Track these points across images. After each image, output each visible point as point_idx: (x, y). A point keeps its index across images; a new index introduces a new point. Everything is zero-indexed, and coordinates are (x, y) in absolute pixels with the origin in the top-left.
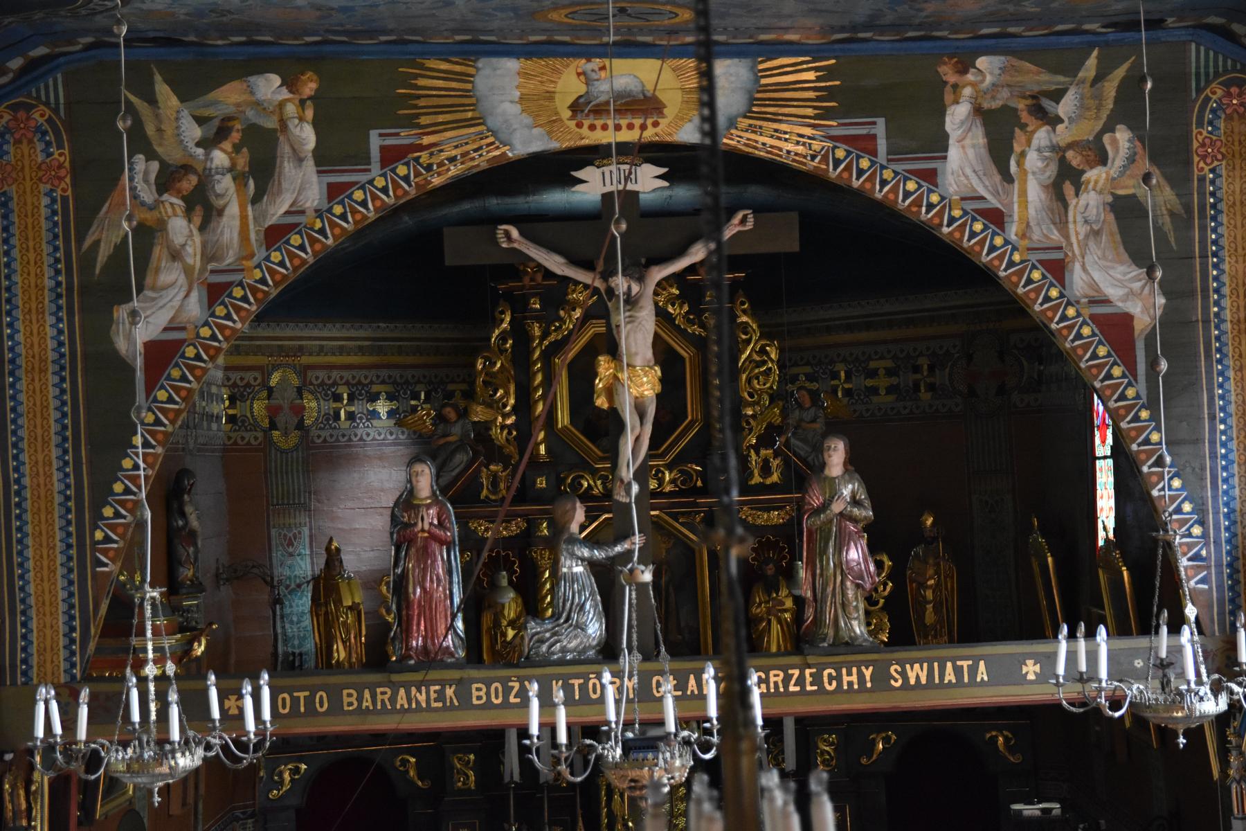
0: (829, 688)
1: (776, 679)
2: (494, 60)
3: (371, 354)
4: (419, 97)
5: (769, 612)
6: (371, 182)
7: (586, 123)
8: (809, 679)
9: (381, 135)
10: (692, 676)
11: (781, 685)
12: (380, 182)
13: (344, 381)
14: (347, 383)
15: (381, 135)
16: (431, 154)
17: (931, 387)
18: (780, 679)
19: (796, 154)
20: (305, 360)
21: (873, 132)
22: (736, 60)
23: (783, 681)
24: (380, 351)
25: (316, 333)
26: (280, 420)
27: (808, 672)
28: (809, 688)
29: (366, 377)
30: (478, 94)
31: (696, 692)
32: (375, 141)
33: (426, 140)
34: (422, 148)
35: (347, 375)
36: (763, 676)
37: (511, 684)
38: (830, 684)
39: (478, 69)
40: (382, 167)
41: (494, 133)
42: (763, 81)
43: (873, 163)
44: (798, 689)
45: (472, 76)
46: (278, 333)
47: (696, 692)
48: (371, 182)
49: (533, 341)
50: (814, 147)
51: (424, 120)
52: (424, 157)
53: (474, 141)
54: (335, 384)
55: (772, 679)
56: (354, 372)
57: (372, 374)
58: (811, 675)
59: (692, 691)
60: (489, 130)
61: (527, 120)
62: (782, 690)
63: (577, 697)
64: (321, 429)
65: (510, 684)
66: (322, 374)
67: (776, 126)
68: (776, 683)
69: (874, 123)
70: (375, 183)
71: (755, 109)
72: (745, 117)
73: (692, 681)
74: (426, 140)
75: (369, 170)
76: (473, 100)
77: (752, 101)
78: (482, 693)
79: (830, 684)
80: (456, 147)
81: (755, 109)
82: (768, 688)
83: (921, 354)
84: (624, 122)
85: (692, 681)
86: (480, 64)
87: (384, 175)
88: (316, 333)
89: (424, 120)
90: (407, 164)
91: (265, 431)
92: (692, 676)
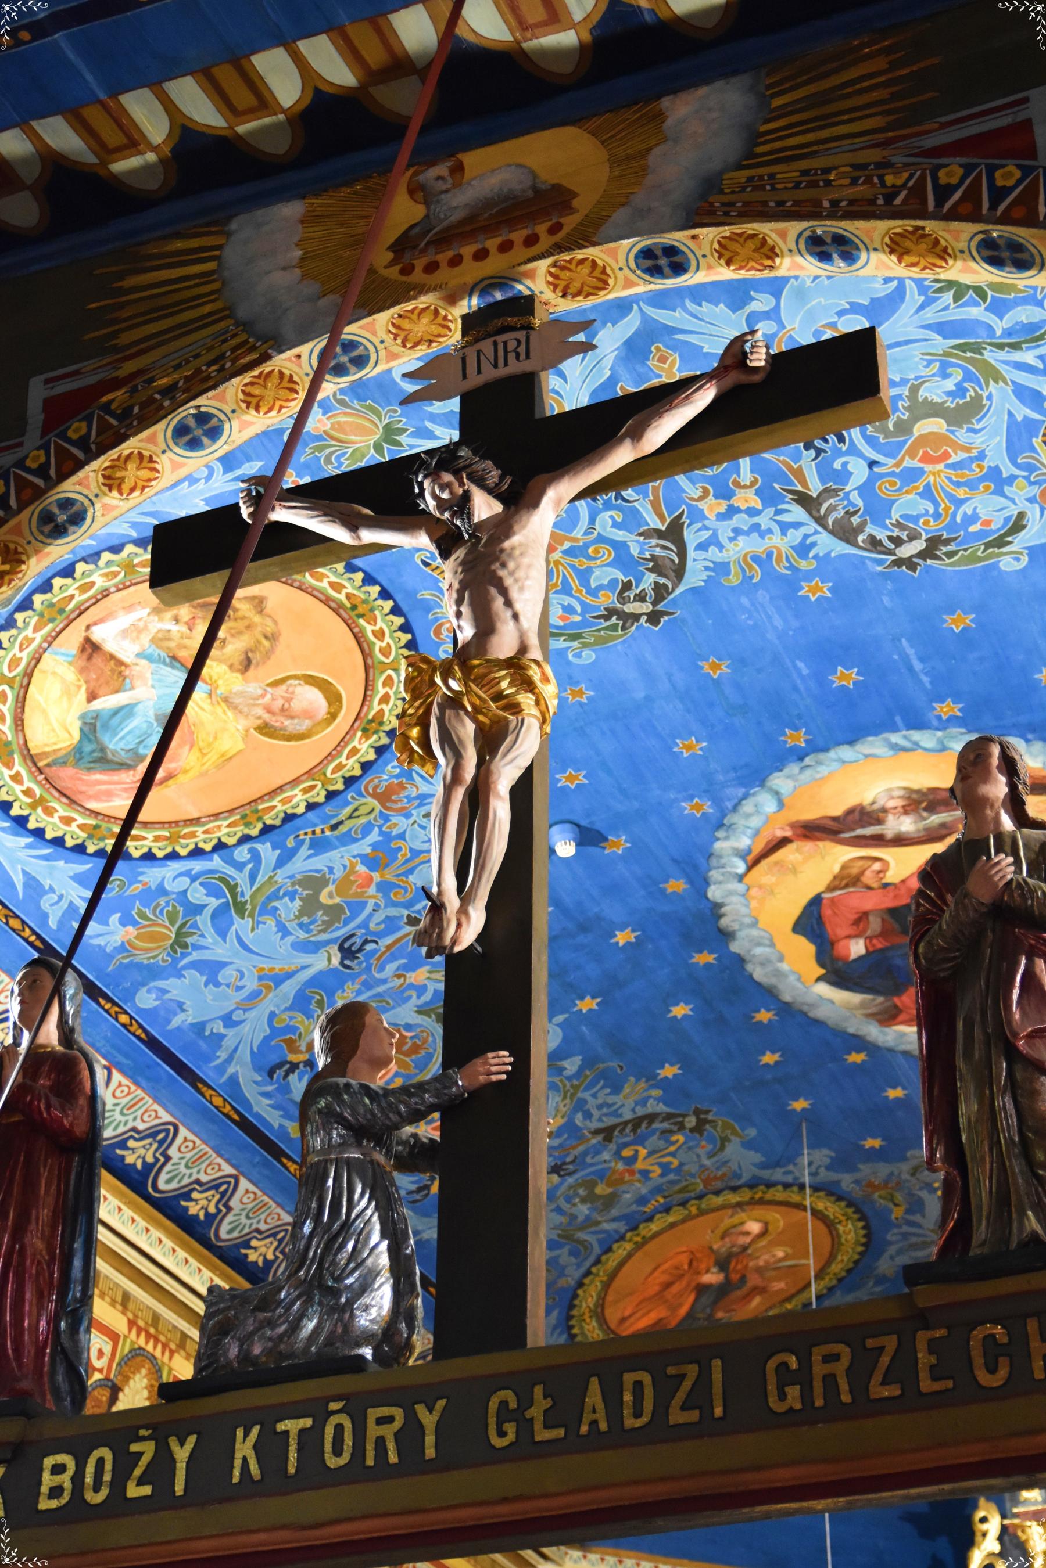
0: (984, 1378)
1: (827, 1368)
2: (259, 214)
4: (122, 306)
6: (21, 464)
7: (420, 264)
8: (924, 1358)
9: (47, 382)
10: (594, 1382)
11: (844, 1385)
12: (36, 459)
15: (47, 382)
16: (134, 390)
18: (840, 1368)
19: (852, 202)
21: (1022, 116)
22: (719, 84)
23: (848, 1371)
27: (922, 1337)
28: (926, 1385)
30: (226, 274)
31: (603, 1426)
32: (37, 392)
33: (129, 367)
34: (115, 384)
36: (793, 1362)
37: (134, 1448)
38: (992, 1370)
39: (229, 235)
40: (44, 433)
41: (246, 326)
42: (777, 102)
43: (1026, 171)
44: (894, 1391)
45: (219, 247)
47: (603, 1426)
48: (21, 464)
50: (889, 180)
51: (125, 338)
52: (118, 396)
53: (210, 349)
55: (819, 1370)
58: (933, 1346)
59: (594, 1423)
60: (237, 324)
61: (311, 288)
62: (846, 1398)
63: (292, 1470)
65: (134, 1448)
67: (804, 164)
68: (830, 1380)
69: (1026, 100)
70: (29, 463)
71: (760, 149)
72: (740, 167)
73: (594, 1395)
74: (129, 367)
75: (21, 444)
76: (216, 286)
77: (754, 138)
78: (65, 1480)
79: (992, 1370)
80: (178, 367)
81: (760, 149)
82: (806, 1396)
84: (492, 244)
85: (594, 1395)
86: (233, 226)
87: (46, 447)
89: (125, 338)
90: (89, 419)
92: (594, 1383)
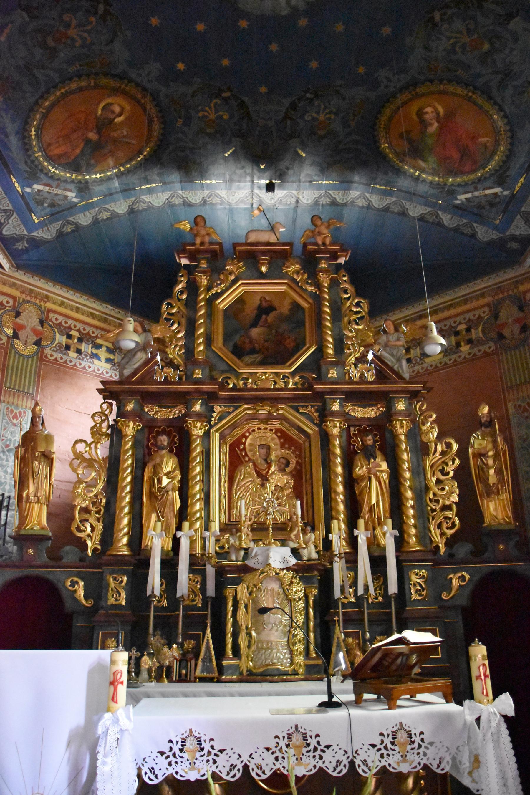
3: (99, 320)
5: (369, 471)
13: (77, 329)
14: (79, 331)
17: (470, 342)
20: (49, 305)
24: (105, 321)
25: (61, 292)
26: (22, 334)
29: (93, 333)
35: (79, 326)
46: (31, 281)
49: (201, 287)
54: (70, 328)
56: (86, 327)
57: (98, 332)
64: (53, 350)
66: (61, 319)
83: (460, 323)
88: (61, 292)
91: (8, 337)
